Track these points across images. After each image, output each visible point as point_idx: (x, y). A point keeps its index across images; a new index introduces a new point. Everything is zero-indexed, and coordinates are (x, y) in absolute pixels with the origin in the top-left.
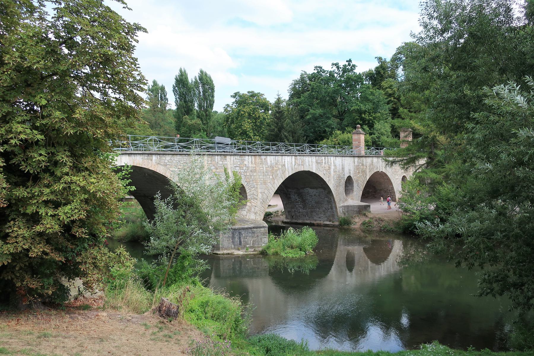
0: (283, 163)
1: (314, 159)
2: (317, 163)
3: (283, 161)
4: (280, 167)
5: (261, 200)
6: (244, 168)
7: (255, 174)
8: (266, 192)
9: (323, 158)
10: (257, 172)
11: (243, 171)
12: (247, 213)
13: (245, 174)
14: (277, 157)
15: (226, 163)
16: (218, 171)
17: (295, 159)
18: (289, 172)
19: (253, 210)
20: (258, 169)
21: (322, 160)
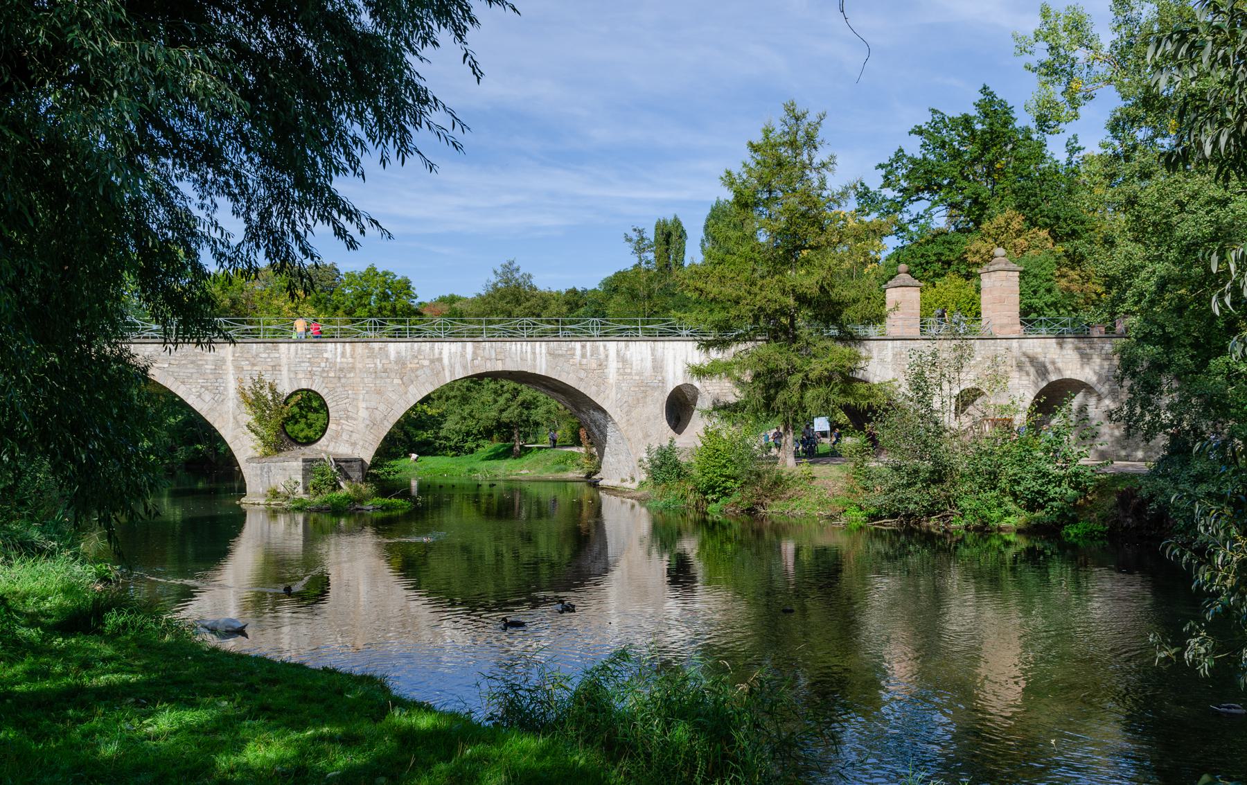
0: (437, 356)
1: (541, 348)
2: (551, 354)
3: (437, 351)
4: (426, 363)
5: (368, 422)
6: (323, 365)
7: (352, 375)
8: (382, 407)
9: (578, 345)
10: (357, 371)
11: (319, 369)
12: (329, 441)
13: (325, 375)
14: (416, 344)
15: (277, 355)
16: (255, 368)
17: (475, 348)
18: (452, 372)
19: (345, 437)
20: (359, 366)
21: (575, 349)
